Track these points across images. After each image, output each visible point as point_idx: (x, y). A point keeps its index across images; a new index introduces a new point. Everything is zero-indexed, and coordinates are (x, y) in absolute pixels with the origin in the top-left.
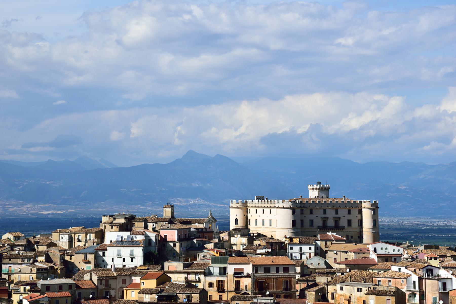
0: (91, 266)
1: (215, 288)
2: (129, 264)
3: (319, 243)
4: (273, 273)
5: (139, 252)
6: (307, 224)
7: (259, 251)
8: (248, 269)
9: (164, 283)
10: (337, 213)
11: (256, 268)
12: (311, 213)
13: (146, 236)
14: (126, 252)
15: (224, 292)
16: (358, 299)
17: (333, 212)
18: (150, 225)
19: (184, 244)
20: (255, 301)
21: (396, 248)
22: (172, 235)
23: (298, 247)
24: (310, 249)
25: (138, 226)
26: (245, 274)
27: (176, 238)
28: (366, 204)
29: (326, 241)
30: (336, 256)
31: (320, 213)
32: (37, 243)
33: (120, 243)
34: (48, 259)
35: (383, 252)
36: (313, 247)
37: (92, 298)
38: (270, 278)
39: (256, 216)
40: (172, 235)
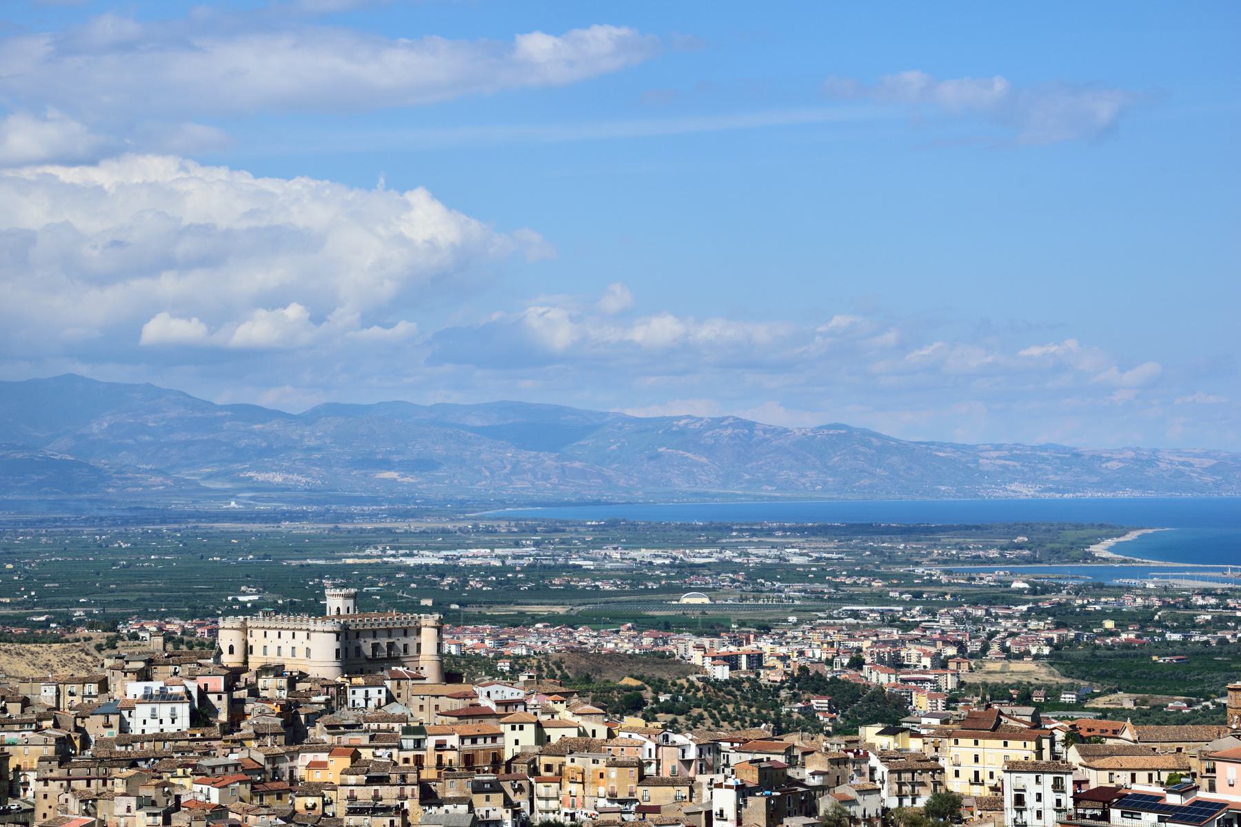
0: (115, 731)
1: (412, 764)
2: (169, 728)
4: (480, 741)
5: (183, 710)
7: (314, 699)
8: (453, 740)
11: (462, 738)
14: (164, 710)
23: (363, 690)
24: (380, 692)
26: (448, 747)
29: (399, 679)
33: (148, 698)
35: (499, 697)
36: (383, 690)
39: (266, 642)
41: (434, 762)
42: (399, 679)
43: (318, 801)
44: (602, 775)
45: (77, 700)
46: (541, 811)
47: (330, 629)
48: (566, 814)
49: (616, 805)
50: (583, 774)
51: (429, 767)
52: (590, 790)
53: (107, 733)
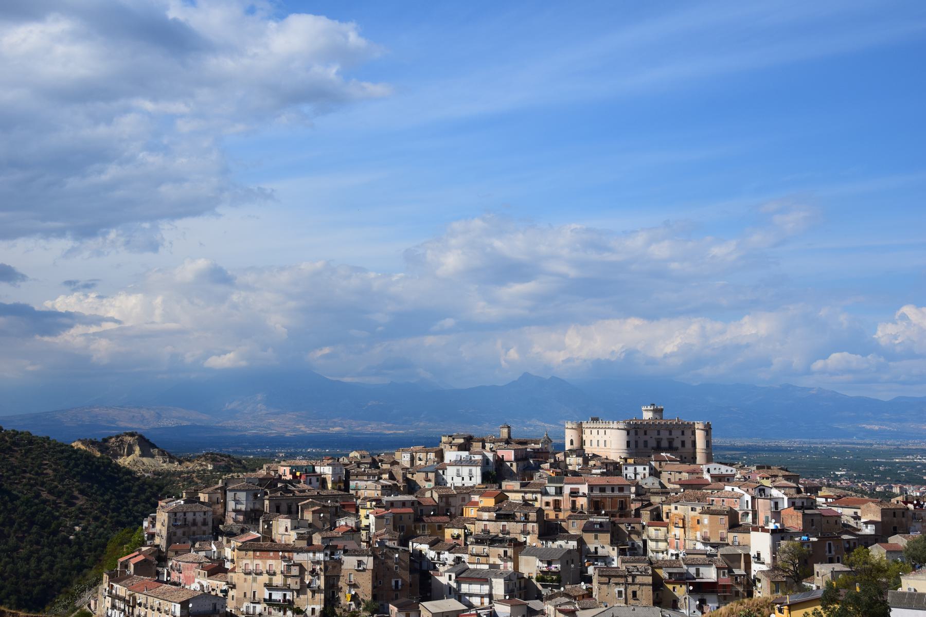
0: (432, 484)
1: (552, 507)
2: (467, 483)
3: (653, 463)
4: (608, 493)
5: (477, 471)
6: (641, 445)
7: (594, 471)
8: (584, 489)
9: (501, 501)
10: (670, 434)
11: (591, 488)
12: (645, 434)
13: (484, 456)
14: (465, 471)
15: (560, 510)
16: (693, 518)
17: (667, 433)
18: (488, 446)
19: (521, 464)
20: (591, 520)
21: (729, 468)
22: (509, 455)
24: (645, 469)
25: (477, 446)
26: (581, 494)
27: (513, 458)
28: (699, 426)
29: (660, 462)
30: (670, 476)
31: (655, 435)
32: (381, 461)
33: (459, 463)
34: (392, 477)
35: (716, 472)
36: (647, 468)
37: (434, 515)
38: (605, 498)
39: (591, 437)
40: (509, 455)
41: (569, 506)
42: (660, 462)
43: (461, 532)
44: (698, 522)
45: (423, 463)
46: (652, 551)
47: (622, 427)
48: (672, 555)
49: (709, 548)
50: (684, 520)
51: (566, 510)
52: (690, 534)
53: (428, 485)
